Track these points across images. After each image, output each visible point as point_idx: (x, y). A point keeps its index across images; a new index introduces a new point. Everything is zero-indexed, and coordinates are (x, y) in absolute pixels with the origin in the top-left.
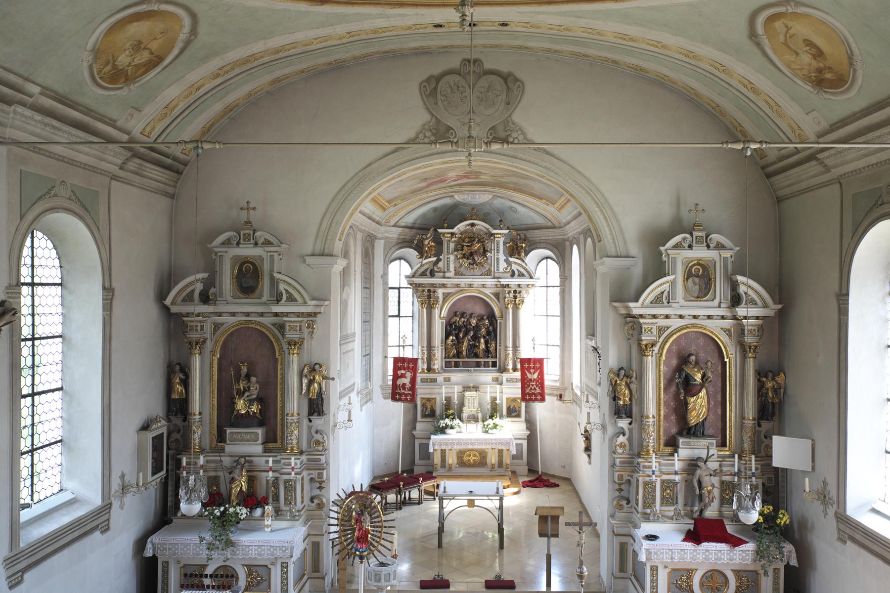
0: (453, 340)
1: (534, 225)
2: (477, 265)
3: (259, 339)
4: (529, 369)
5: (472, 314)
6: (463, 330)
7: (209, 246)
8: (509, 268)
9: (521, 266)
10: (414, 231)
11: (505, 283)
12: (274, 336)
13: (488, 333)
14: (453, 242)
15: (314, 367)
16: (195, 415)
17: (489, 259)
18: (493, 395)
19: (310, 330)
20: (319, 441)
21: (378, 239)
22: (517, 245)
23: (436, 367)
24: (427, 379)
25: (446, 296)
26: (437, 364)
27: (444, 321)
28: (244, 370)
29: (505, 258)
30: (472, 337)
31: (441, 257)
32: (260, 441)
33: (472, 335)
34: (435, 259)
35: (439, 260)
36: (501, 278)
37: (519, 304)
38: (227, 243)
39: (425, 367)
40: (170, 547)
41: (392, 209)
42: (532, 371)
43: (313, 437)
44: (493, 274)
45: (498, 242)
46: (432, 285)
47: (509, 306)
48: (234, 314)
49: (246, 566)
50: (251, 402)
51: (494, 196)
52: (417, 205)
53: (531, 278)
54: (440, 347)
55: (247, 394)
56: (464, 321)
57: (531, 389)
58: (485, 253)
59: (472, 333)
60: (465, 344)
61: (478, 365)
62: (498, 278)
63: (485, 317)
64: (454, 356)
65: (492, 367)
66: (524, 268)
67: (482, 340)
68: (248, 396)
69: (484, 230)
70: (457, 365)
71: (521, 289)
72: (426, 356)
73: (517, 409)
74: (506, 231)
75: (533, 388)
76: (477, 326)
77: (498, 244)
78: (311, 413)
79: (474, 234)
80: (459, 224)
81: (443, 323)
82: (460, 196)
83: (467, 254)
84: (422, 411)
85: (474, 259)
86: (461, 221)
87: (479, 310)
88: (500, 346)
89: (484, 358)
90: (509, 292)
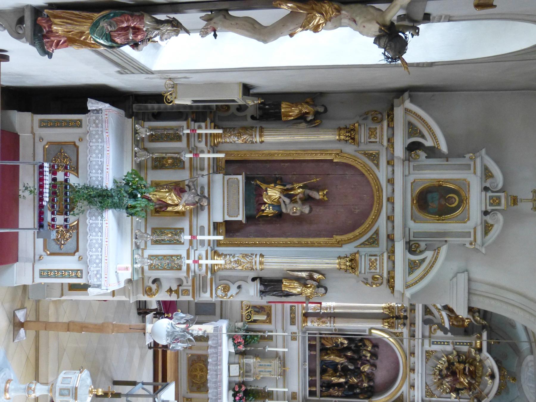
0: (342, 344)
2: (439, 379)
3: (357, 211)
7: (484, 151)
12: (361, 235)
13: (352, 387)
15: (322, 287)
16: (261, 136)
17: (448, 395)
19: (370, 280)
20: (228, 291)
23: (309, 324)
24: (295, 313)
25: (398, 336)
26: (312, 324)
27: (367, 333)
28: (318, 196)
30: (346, 366)
31: (449, 334)
32: (228, 218)
33: (350, 367)
34: (447, 325)
35: (445, 331)
38: (487, 174)
40: (100, 148)
43: (233, 283)
46: (413, 324)
48: (391, 181)
49: (78, 224)
50: (277, 205)
55: (287, 201)
56: (366, 357)
59: (351, 367)
60: (338, 360)
61: (312, 372)
63: (372, 384)
64: (322, 344)
65: (310, 391)
67: (342, 380)
68: (284, 202)
69: (486, 391)
70: (311, 347)
78: (264, 281)
79: (481, 377)
81: (365, 331)
83: (454, 368)
85: (447, 376)
86: (497, 362)
87: (381, 376)
89: (321, 381)
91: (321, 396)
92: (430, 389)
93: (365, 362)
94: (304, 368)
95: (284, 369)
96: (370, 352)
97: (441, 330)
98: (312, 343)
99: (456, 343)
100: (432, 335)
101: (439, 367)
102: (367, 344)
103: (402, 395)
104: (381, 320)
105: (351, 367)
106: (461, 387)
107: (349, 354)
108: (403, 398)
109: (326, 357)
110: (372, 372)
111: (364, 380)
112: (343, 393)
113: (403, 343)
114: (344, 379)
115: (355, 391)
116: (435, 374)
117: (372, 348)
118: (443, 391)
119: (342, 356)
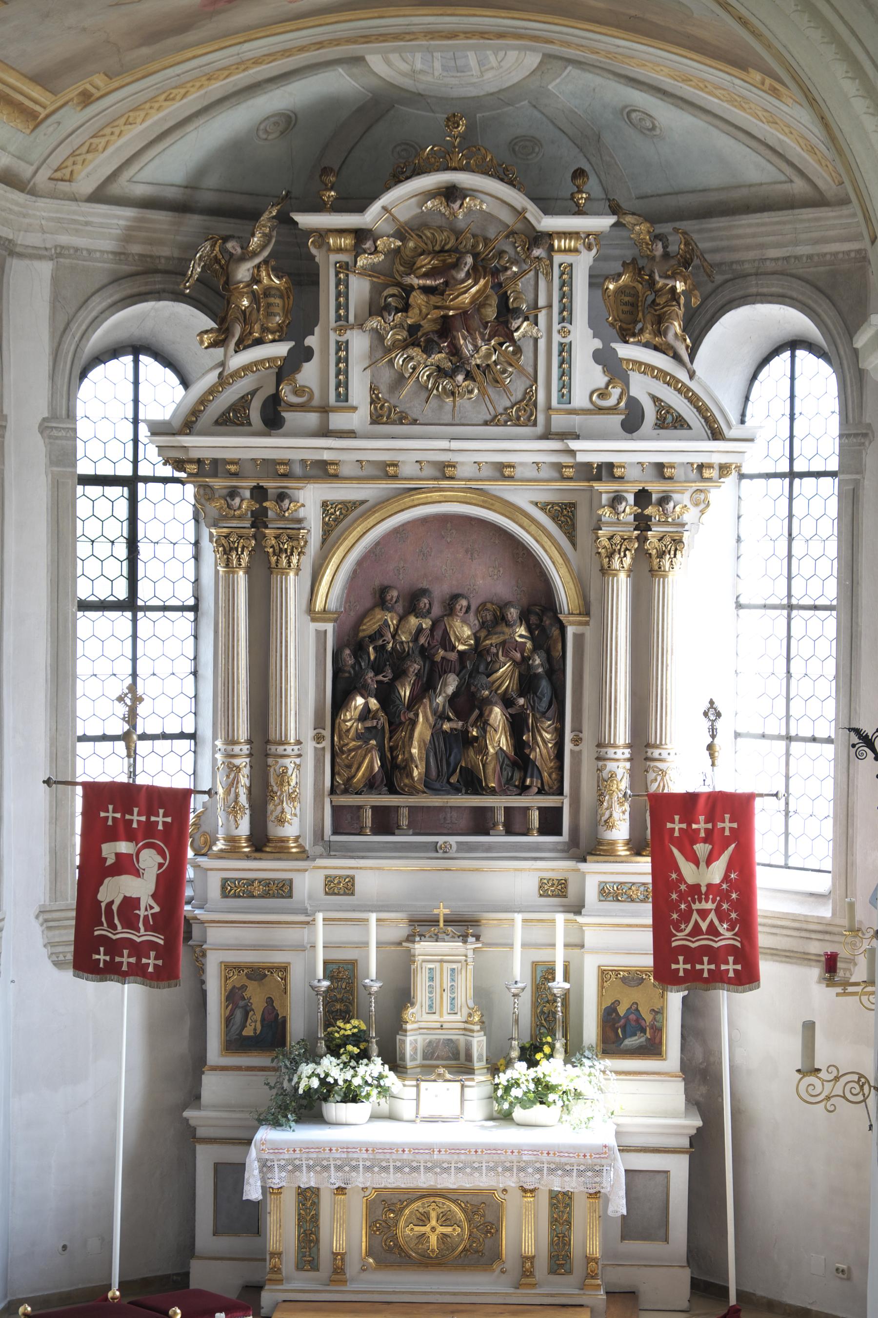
0: (366, 714)
1: (736, 195)
2: (469, 376)
4: (687, 841)
5: (455, 598)
6: (415, 667)
8: (615, 392)
9: (671, 381)
10: (194, 221)
11: (596, 459)
14: (365, 272)
17: (527, 348)
18: (541, 955)
21: (20, 255)
22: (652, 283)
23: (290, 830)
24: (251, 882)
27: (329, 627)
29: (598, 344)
30: (452, 700)
31: (311, 341)
33: (450, 689)
34: (281, 349)
35: (301, 354)
36: (577, 437)
37: (661, 555)
39: (244, 828)
41: (72, 117)
42: (702, 849)
44: (541, 419)
45: (568, 270)
47: (616, 563)
51: (548, 57)
52: (194, 100)
53: (716, 434)
54: (310, 747)
56: (420, 630)
57: (697, 927)
58: (506, 324)
59: (451, 685)
60: (422, 730)
62: (563, 436)
63: (513, 613)
64: (371, 785)
65: (542, 832)
66: (684, 391)
67: (497, 715)
69: (506, 216)
72: (244, 781)
73: (648, 1017)
74: (603, 223)
75: (704, 926)
76: (478, 651)
77: (567, 283)
79: (458, 234)
80: (387, 188)
81: (321, 636)
82: (394, 58)
83: (427, 326)
84: (228, 1021)
85: (455, 351)
86: (399, 178)
88: (577, 741)
89: (504, 792)
90: (616, 499)
91: (561, 793)
92: (506, 409)
93: (438, 634)
94: (457, 851)
95: (441, 924)
96: (402, 618)
97: (297, 369)
98: (536, 823)
99: (339, 318)
100: (316, 402)
101: (429, 377)
102: (376, 627)
103: (544, 507)
104: (276, 578)
105: (451, 685)
106: (494, 301)
107: (406, 692)
108: (553, 504)
109: (416, 773)
110: (478, 611)
111: (502, 638)
112: (544, 714)
113: (363, 502)
114: (491, 711)
115: (540, 670)
116: (453, 394)
117: (389, 610)
118: (511, 365)
119: (411, 715)
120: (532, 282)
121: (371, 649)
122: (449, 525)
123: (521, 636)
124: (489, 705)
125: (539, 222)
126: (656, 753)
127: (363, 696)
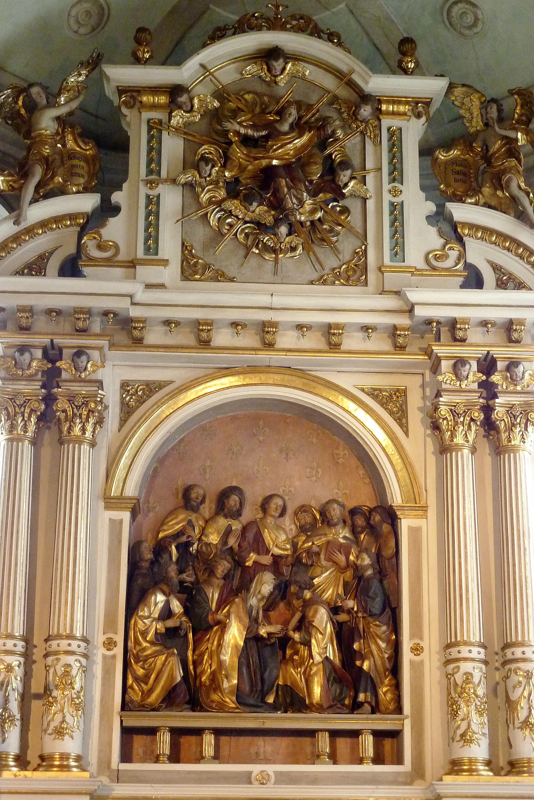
8: (454, 254)
17: (354, 206)
29: (431, 207)
31: (117, 197)
47: (459, 440)
71: (513, 352)
80: (204, 45)
88: (417, 650)
91: (399, 710)
93: (250, 536)
97: (103, 224)
99: (150, 172)
100: (122, 256)
110: (296, 514)
114: (316, 612)
116: (274, 251)
120: (359, 147)
121: (173, 547)
122: (261, 423)
123: (345, 538)
124: (313, 604)
125: (367, 82)
126: (518, 652)
127: (164, 593)
